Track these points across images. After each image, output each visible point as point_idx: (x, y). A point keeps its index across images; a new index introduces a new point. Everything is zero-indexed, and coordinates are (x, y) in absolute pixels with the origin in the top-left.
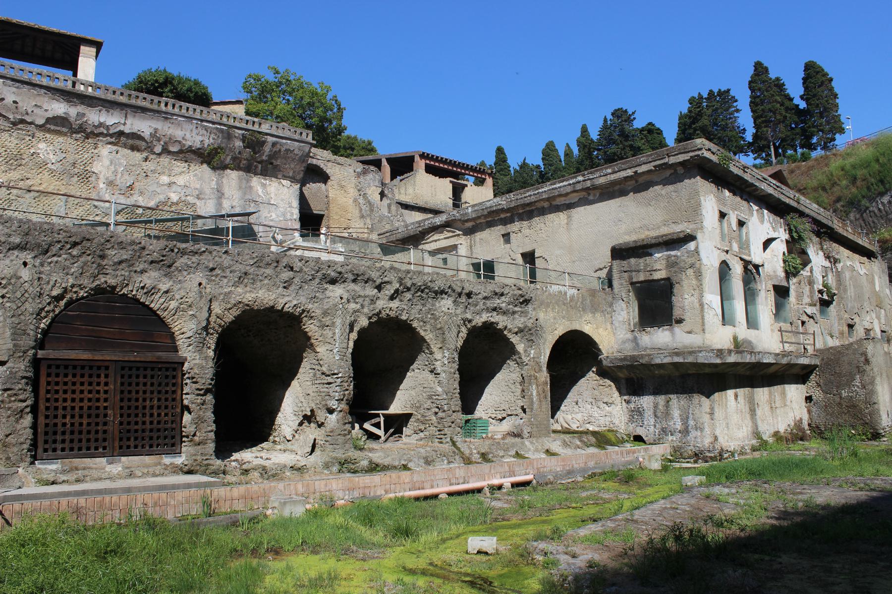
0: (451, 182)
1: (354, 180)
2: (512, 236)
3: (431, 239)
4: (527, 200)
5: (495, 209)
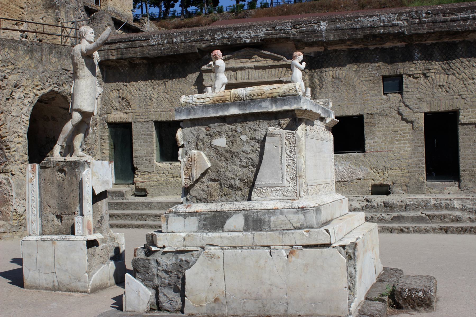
2: (408, 82)
5: (382, 31)
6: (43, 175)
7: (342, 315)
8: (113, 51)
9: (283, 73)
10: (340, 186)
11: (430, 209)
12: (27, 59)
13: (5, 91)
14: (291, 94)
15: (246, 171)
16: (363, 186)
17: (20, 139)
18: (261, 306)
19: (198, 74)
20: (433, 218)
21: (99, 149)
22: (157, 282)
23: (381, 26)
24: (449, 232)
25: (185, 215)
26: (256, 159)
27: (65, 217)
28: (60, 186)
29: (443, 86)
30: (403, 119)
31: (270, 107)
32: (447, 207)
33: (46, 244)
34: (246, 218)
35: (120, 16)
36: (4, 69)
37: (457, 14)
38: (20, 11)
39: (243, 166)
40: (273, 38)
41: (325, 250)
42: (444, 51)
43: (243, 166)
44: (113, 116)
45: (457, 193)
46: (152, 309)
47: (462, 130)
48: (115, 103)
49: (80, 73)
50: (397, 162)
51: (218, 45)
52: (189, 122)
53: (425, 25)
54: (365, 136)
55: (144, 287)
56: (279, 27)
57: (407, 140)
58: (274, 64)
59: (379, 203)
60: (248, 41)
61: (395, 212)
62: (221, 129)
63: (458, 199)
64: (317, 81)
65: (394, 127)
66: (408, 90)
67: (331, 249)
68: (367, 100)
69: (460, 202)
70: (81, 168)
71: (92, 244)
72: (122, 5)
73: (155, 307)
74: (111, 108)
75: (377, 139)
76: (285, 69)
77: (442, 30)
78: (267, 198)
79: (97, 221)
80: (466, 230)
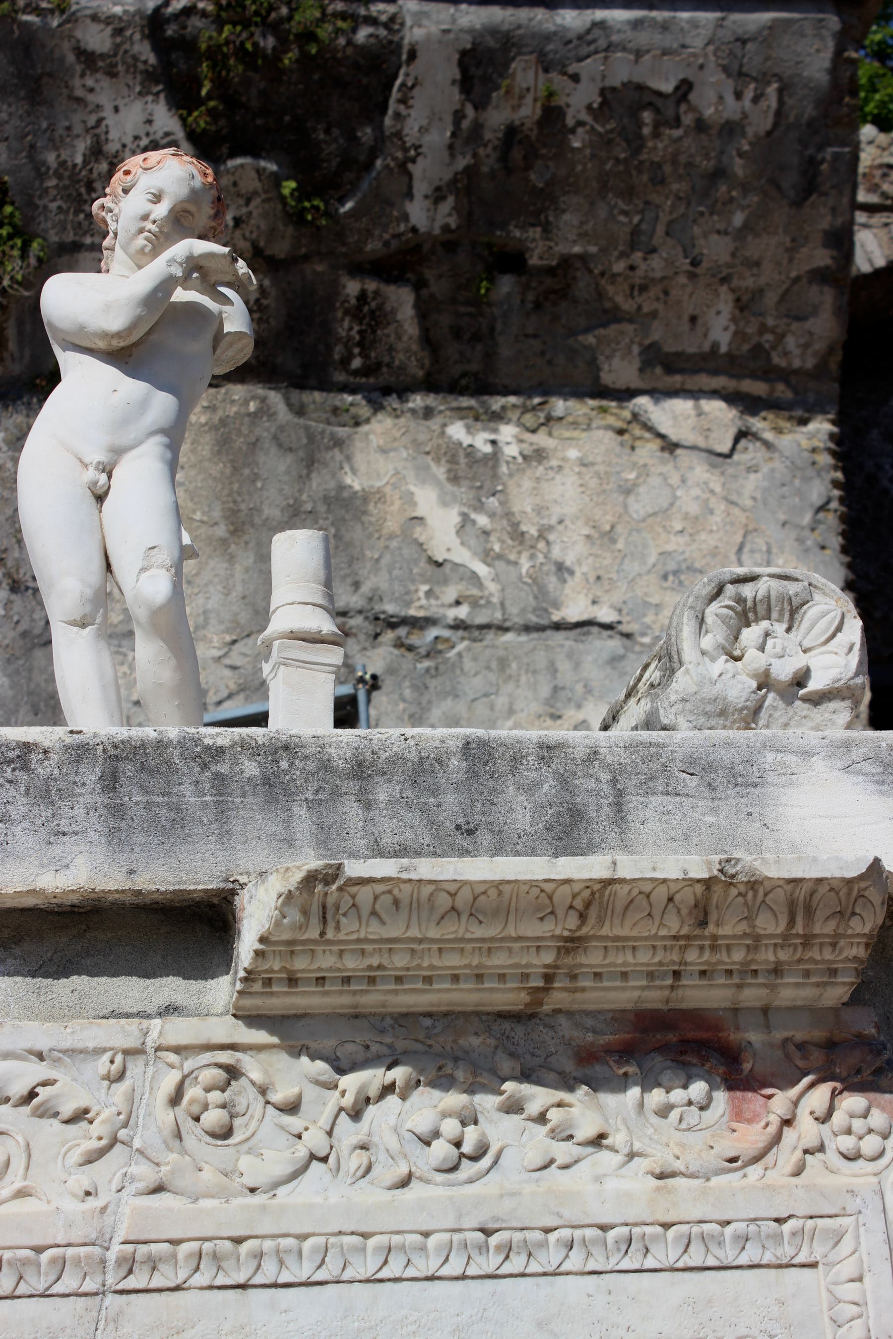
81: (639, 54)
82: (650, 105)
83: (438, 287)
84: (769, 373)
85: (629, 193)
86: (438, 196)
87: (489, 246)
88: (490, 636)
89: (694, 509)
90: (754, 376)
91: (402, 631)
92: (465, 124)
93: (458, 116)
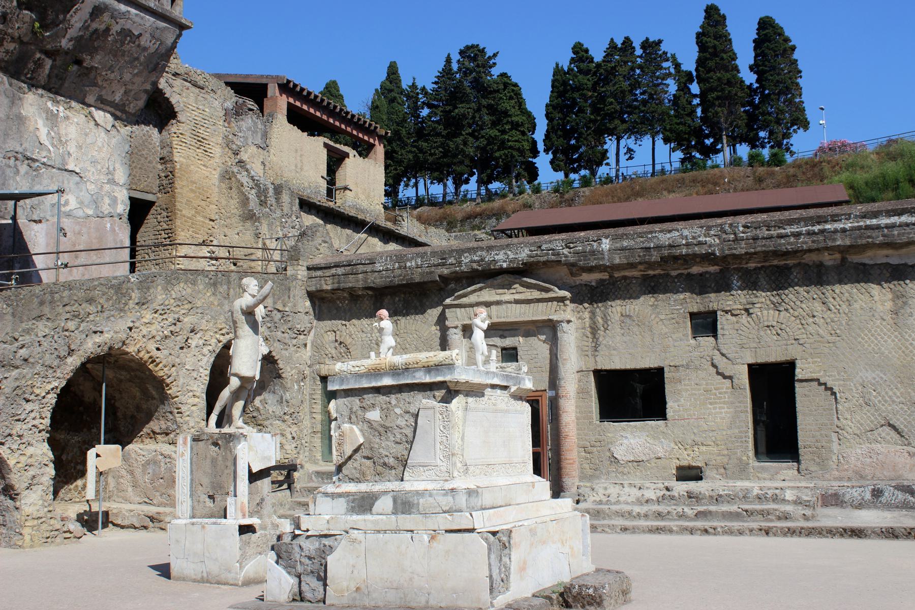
0: (326, 145)
1: (221, 128)
2: (723, 321)
3: (473, 299)
4: (786, 245)
5: (684, 251)
6: (195, 448)
7: (483, 608)
8: (328, 279)
9: (553, 310)
10: (632, 468)
11: (751, 502)
12: (208, 294)
13: (178, 338)
14: (447, 363)
15: (401, 447)
16: (664, 468)
17: (196, 400)
18: (402, 596)
19: (440, 309)
20: (752, 514)
21: (308, 413)
22: (300, 569)
23: (683, 245)
24: (771, 534)
25: (334, 496)
26: (410, 435)
27: (218, 498)
28: (214, 461)
29: (773, 327)
30: (718, 373)
31: (423, 377)
32: (775, 499)
33: (195, 528)
34: (395, 501)
35: (364, 212)
36: (178, 309)
37: (786, 227)
38: (209, 224)
39: (397, 443)
40: (539, 262)
41: (467, 535)
42: (773, 278)
43: (397, 443)
44: (327, 367)
45: (795, 480)
46: (294, 600)
47: (799, 389)
48: (330, 349)
49: (240, 332)
50: (711, 435)
51: (466, 270)
52: (342, 392)
53: (743, 242)
54: (667, 397)
55: (286, 575)
56: (547, 246)
57: (724, 403)
58: (541, 297)
59: (682, 493)
60: (505, 265)
61: (702, 505)
62: (375, 401)
63: (792, 488)
64: (600, 320)
65: (707, 384)
66: (725, 333)
67: (474, 535)
68: (668, 347)
69: (795, 492)
70: (236, 441)
71: (245, 529)
72: (368, 197)
73: (298, 598)
74: (325, 356)
75: (683, 401)
76: (555, 303)
77: (767, 249)
78: (419, 479)
79: (255, 503)
80: (794, 532)
81: (134, 23)
82: (130, 36)
83: (58, 63)
84: (123, 111)
85: (115, 56)
86: (71, 40)
87: (76, 57)
88: (50, 168)
89: (100, 145)
90: (119, 110)
91: (30, 161)
92: (86, 24)
93: (86, 21)
